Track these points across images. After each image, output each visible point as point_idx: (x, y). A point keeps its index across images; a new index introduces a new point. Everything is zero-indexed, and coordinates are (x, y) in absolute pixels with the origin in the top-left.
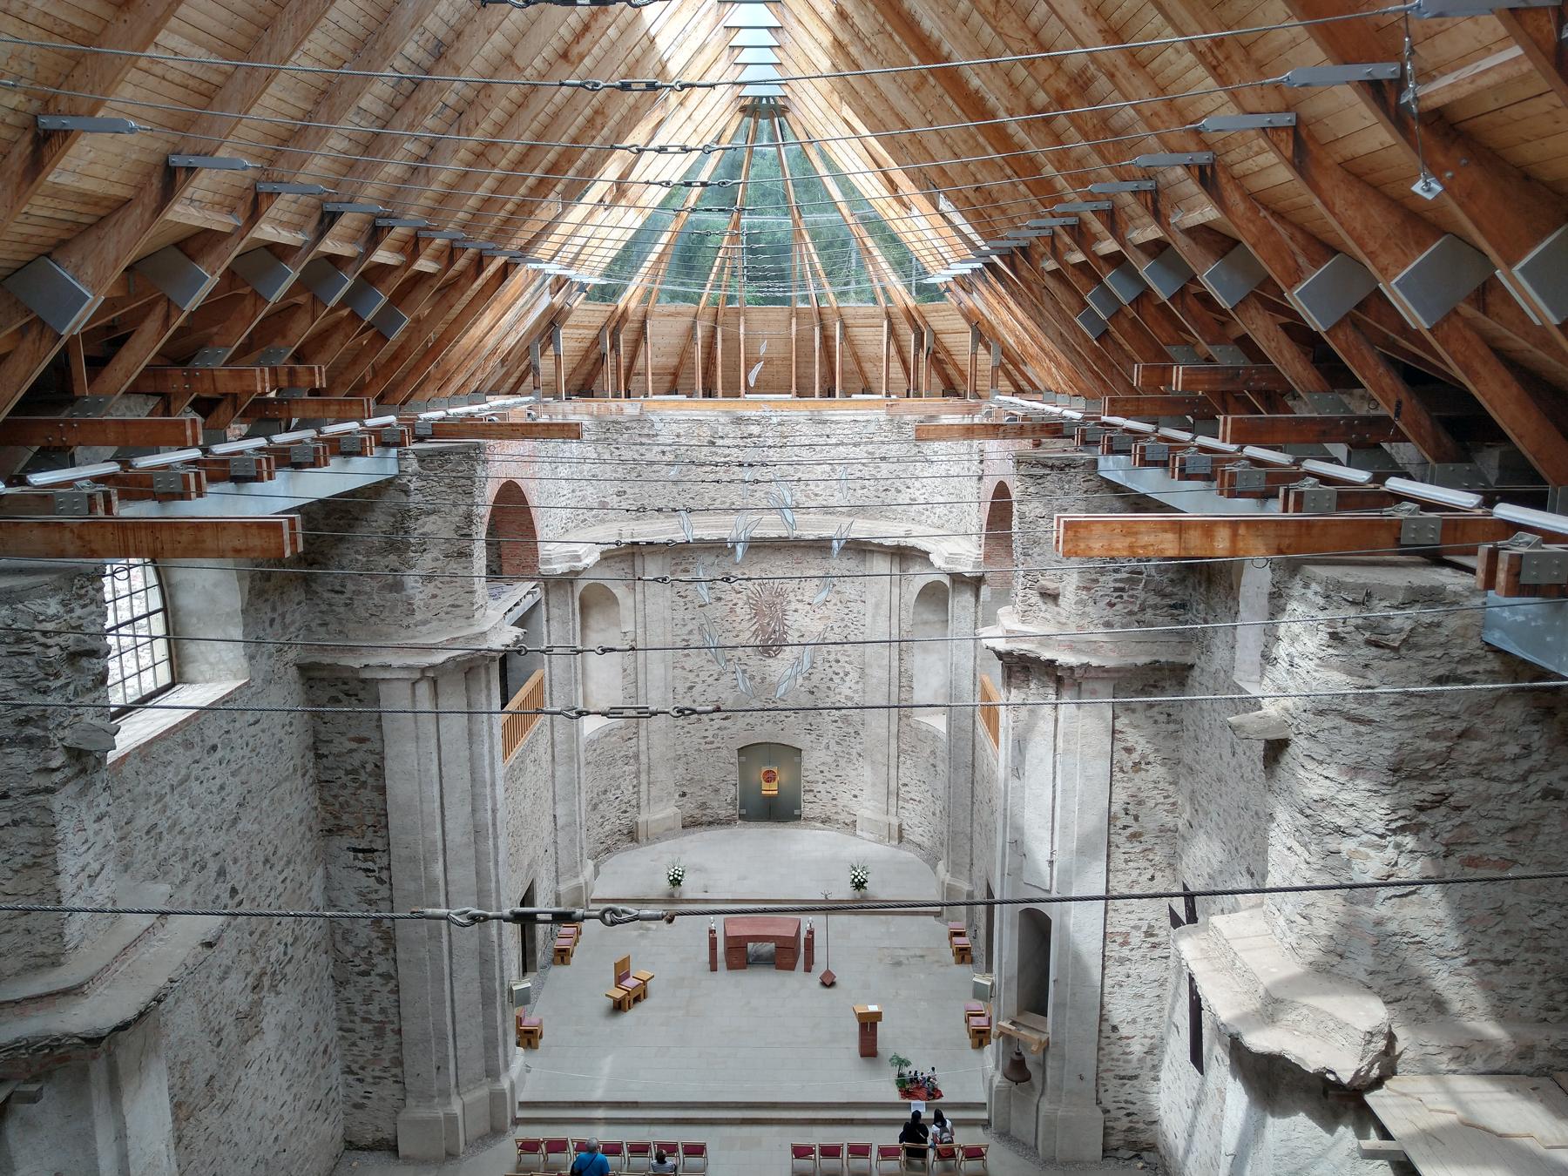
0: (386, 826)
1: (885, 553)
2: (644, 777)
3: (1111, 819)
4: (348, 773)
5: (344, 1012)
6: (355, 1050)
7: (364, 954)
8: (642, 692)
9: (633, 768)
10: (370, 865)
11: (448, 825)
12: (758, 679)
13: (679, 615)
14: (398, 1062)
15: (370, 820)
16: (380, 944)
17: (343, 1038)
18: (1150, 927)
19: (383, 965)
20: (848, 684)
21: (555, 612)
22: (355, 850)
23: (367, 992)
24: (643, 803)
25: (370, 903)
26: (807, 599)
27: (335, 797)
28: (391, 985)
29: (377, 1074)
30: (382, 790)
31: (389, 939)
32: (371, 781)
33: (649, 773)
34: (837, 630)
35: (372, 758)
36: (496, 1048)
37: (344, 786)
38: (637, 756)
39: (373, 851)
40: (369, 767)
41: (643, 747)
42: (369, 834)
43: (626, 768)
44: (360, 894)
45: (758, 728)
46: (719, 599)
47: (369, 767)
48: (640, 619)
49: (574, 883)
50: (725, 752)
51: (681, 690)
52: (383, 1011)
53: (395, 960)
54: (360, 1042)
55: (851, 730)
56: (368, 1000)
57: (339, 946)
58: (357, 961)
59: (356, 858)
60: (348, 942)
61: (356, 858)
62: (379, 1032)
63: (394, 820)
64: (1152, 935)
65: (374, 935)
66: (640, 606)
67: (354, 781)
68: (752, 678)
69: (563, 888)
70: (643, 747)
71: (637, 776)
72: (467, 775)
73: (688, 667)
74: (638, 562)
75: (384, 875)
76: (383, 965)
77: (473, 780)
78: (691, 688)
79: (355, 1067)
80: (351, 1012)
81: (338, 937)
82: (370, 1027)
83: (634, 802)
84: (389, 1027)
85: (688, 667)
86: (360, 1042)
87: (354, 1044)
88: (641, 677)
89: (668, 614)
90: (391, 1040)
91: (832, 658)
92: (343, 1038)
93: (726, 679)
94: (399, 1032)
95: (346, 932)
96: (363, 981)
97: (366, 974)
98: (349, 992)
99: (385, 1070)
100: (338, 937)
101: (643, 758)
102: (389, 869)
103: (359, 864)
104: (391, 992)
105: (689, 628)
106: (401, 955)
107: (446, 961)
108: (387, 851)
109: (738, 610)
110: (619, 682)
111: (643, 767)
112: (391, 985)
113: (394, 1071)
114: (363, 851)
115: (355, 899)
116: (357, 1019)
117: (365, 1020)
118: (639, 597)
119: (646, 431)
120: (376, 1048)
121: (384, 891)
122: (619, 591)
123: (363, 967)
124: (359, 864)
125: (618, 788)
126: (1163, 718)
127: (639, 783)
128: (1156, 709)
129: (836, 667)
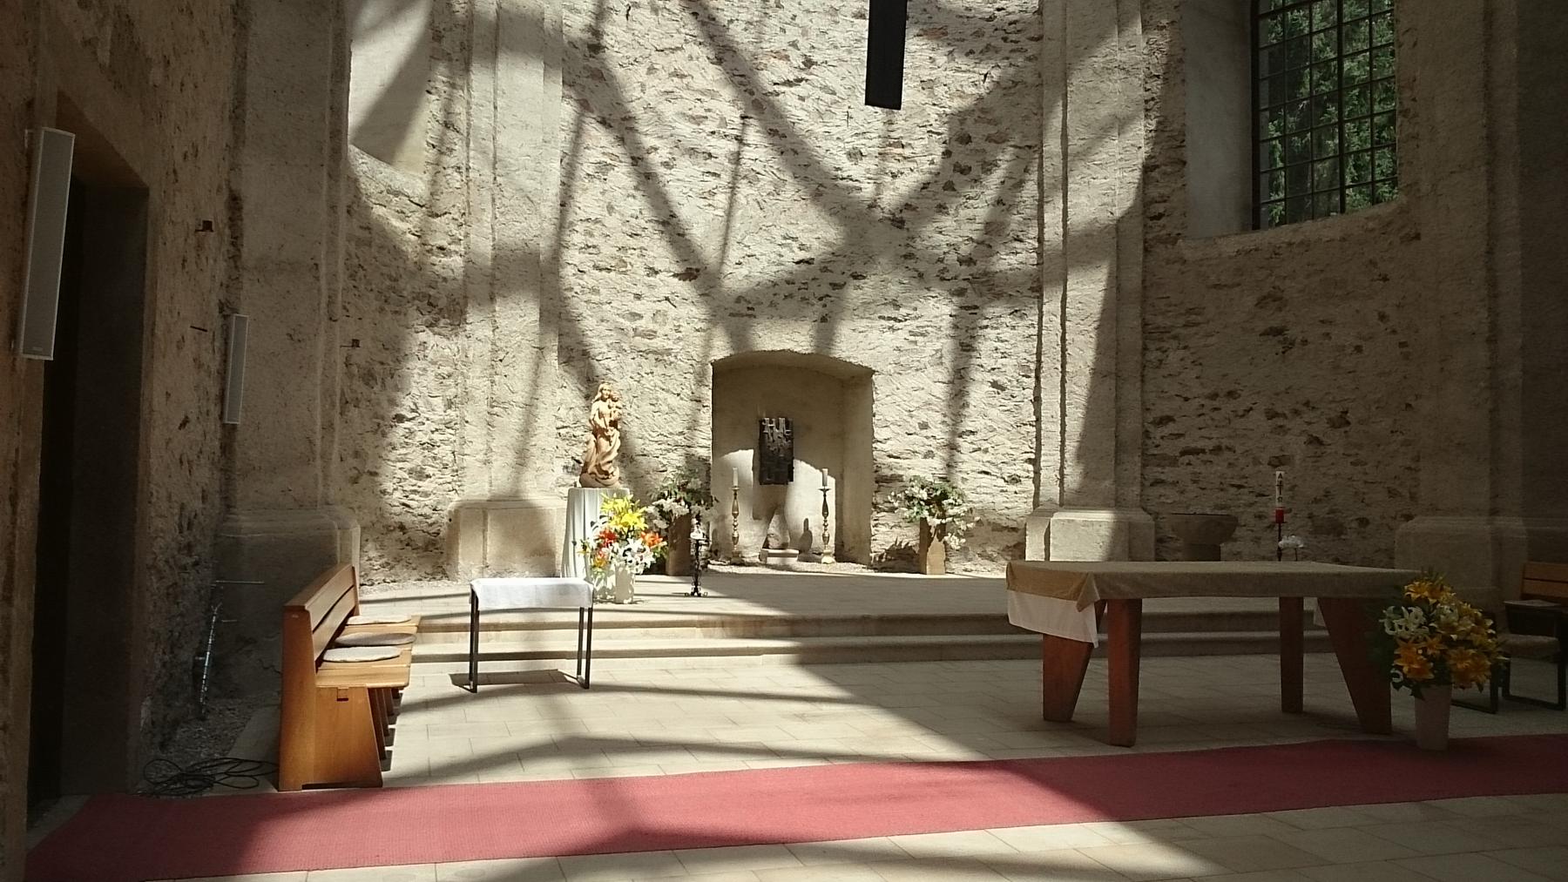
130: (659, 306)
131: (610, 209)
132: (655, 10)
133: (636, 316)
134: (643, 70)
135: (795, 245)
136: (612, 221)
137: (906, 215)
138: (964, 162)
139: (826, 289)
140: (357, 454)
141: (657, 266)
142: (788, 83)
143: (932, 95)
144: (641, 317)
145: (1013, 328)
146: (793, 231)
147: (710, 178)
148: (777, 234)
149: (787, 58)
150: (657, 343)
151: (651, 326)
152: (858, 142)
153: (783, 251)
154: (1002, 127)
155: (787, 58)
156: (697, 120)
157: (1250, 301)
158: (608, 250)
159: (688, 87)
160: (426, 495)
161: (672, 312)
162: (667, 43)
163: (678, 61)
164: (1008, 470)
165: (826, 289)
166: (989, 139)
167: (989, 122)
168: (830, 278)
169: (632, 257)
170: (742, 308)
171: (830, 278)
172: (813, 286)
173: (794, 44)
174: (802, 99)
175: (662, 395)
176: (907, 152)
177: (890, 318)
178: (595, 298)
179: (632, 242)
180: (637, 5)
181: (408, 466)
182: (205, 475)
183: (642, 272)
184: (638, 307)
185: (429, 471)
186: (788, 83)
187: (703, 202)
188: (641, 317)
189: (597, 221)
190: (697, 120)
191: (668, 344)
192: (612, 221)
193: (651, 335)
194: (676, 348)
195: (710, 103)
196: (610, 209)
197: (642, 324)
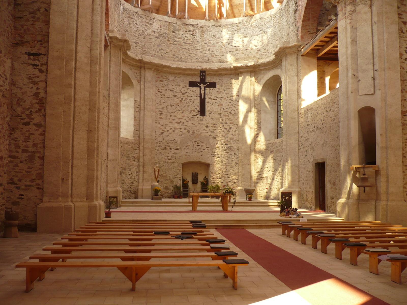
0: (48, 41)
1: (247, 72)
2: (141, 169)
3: (401, 55)
4: (31, 13)
5: (13, 146)
6: (17, 169)
7: (28, 112)
8: (142, 129)
9: (137, 164)
10: (37, 62)
11: (79, 48)
12: (191, 133)
13: (159, 99)
14: (41, 176)
15: (39, 38)
16: (37, 106)
17: (11, 162)
19: (37, 119)
20: (231, 133)
21: (113, 58)
22: (30, 54)
23: (27, 135)
24: (141, 181)
25: (35, 83)
26: (213, 97)
27: (22, 26)
28: (41, 131)
29: (28, 183)
30: (47, 23)
31: (42, 103)
32: (42, 18)
33: (143, 167)
34: (226, 110)
35: (44, 6)
36: (92, 182)
37: (28, 20)
38: (138, 158)
39: (38, 54)
40: (42, 10)
41: (141, 155)
42: (38, 46)
43: (134, 162)
44: (29, 78)
45: (191, 155)
46: (175, 96)
47: (42, 10)
48: (142, 96)
49: (114, 189)
50: (176, 164)
51: (158, 133)
52: (35, 145)
53: (44, 116)
54: (20, 164)
55: (233, 153)
56: (27, 139)
57: (14, 107)
58: (24, 116)
59: (29, 58)
60: (19, 104)
61: (29, 58)
62: (31, 159)
63: (53, 37)
65: (34, 101)
66: (142, 90)
67: (33, 17)
68: (189, 132)
69: (110, 189)
70: (141, 155)
71: (139, 166)
72: (90, 28)
73: (162, 123)
74: (143, 72)
75: (44, 68)
76: (37, 119)
77: (92, 33)
78: (162, 133)
79: (16, 179)
80: (17, 146)
81: (15, 102)
82: (26, 155)
83: (136, 179)
84: (37, 155)
85: (161, 123)
86: (20, 164)
87: (17, 165)
88: (142, 122)
89: (154, 97)
90: (37, 162)
91: (224, 122)
92: (11, 162)
93: (177, 131)
94: (42, 158)
95: (19, 99)
96: (25, 128)
97: (27, 124)
98: (17, 134)
99: (33, 181)
100: (15, 102)
101: (141, 160)
102: (46, 64)
103: (30, 62)
104: (41, 134)
105: (163, 106)
106: (48, 111)
107: (72, 118)
108: (46, 54)
109: (183, 101)
110: (132, 122)
111: (141, 164)
112: (41, 131)
113: (38, 181)
114: (34, 55)
115: (26, 81)
116: (20, 150)
117: (24, 151)
118: (142, 87)
119: (148, 21)
120: (29, 168)
121: (43, 77)
122: (134, 82)
123: (27, 120)
124: (30, 62)
125: (130, 170)
127: (139, 171)
129: (226, 126)
130: (172, 155)
131: (164, 139)
132: (171, 106)
133: (168, 156)
134: (169, 116)
135: (196, 143)
136: (164, 141)
137: (216, 137)
138: (226, 127)
139: (202, 150)
140: (123, 180)
141: (172, 148)
142: (195, 115)
143: (220, 116)
144: (169, 156)
145: (234, 156)
146: (196, 140)
147: (181, 133)
148: (193, 141)
149: (195, 111)
150: (172, 161)
151: (171, 158)
152: (207, 125)
153: (194, 144)
154: (232, 121)
155: (195, 111)
156: (179, 123)
157: (269, 152)
158: (163, 146)
159: (177, 118)
160: (134, 186)
161: (175, 155)
162: (174, 111)
163: (176, 114)
164: (234, 181)
165: (202, 150)
166: (230, 123)
167: (230, 120)
168: (203, 148)
169: (167, 147)
170: (187, 154)
171: (203, 148)
172: (200, 150)
173: (196, 109)
174: (198, 118)
175: (172, 169)
176: (216, 126)
177: (213, 155)
178: (161, 154)
179: (167, 144)
180: (168, 106)
181: (131, 182)
182: (105, 184)
183: (169, 149)
184: (168, 155)
185: (134, 182)
186: (195, 115)
187: (180, 137)
188: (169, 156)
189: (161, 142)
190: (179, 123)
191: (174, 161)
192: (164, 141)
193: (170, 159)
194: (175, 161)
195: (181, 120)
196: (164, 139)
197: (169, 158)
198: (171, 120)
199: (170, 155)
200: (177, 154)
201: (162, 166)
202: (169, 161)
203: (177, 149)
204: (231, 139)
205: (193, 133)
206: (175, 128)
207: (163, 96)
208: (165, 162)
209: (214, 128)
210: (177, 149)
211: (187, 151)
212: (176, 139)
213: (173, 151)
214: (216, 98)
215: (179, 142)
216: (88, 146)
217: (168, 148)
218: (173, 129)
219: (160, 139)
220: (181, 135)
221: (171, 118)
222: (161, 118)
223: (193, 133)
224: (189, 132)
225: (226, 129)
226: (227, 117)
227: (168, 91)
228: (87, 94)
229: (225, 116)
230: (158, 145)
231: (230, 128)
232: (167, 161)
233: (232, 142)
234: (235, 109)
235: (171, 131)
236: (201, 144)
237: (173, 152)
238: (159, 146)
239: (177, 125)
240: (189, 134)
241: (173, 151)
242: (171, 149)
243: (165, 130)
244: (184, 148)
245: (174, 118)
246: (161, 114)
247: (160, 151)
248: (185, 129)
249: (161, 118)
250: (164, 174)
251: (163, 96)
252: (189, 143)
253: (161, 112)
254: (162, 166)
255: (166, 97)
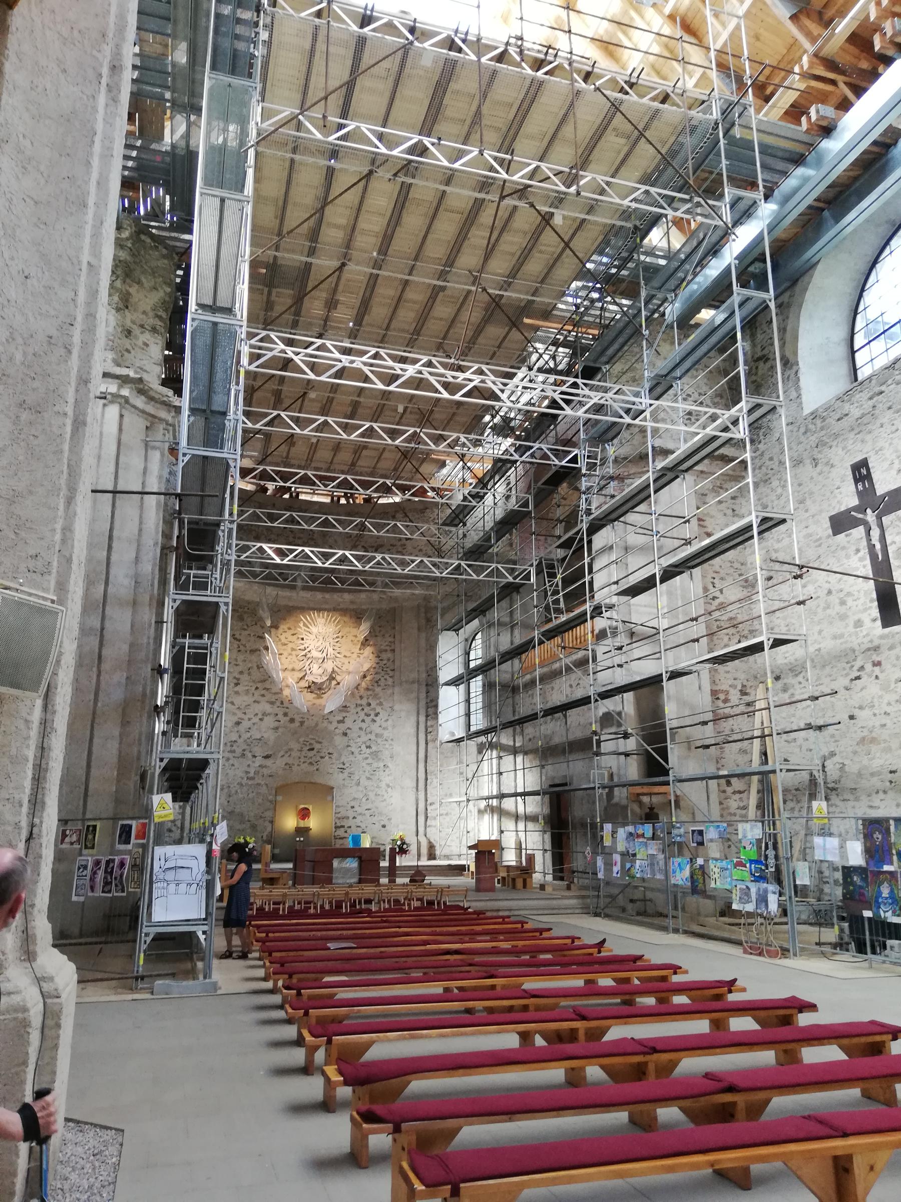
18: (743, 686)
20: (377, 724)
45: (295, 768)
50: (264, 790)
55: (381, 765)
64: (746, 694)
68: (292, 720)
83: (179, 823)
91: (364, 702)
126: (730, 512)
128: (723, 505)
129: (367, 709)
133: (247, 772)
148: (301, 740)
150: (257, 781)
158: (239, 751)
169: (246, 753)
190: (272, 703)
195: (277, 697)
197: (252, 775)
198: (256, 697)
199: (252, 771)
200: (265, 767)
201: (233, 792)
202: (250, 782)
203: (267, 757)
204: (377, 735)
205: (302, 723)
206: (264, 714)
207: (242, 648)
208: (241, 784)
209: (344, 714)
210: (267, 757)
211: (290, 762)
212: (266, 735)
213: (259, 761)
214: (348, 654)
215: (271, 743)
216: (120, 752)
217: (250, 755)
218: (260, 716)
219: (234, 737)
220: (277, 728)
221: (257, 693)
222: (237, 693)
223: (302, 723)
224: (292, 720)
225: (368, 715)
226: (369, 693)
227: (252, 639)
228: (125, 648)
229: (367, 689)
230: (229, 748)
231: (377, 715)
232: (245, 781)
233: (379, 740)
234: (387, 677)
235: (256, 720)
236: (317, 746)
237: (257, 764)
238: (231, 752)
239: (268, 708)
240: (292, 725)
241: (259, 761)
242: (254, 756)
243: (243, 716)
244: (282, 753)
245: (263, 692)
246: (237, 684)
247: (231, 762)
248: (285, 715)
249: (237, 693)
250: (237, 810)
251: (242, 648)
252: (294, 745)
253: (238, 679)
254: (233, 792)
255: (248, 648)
